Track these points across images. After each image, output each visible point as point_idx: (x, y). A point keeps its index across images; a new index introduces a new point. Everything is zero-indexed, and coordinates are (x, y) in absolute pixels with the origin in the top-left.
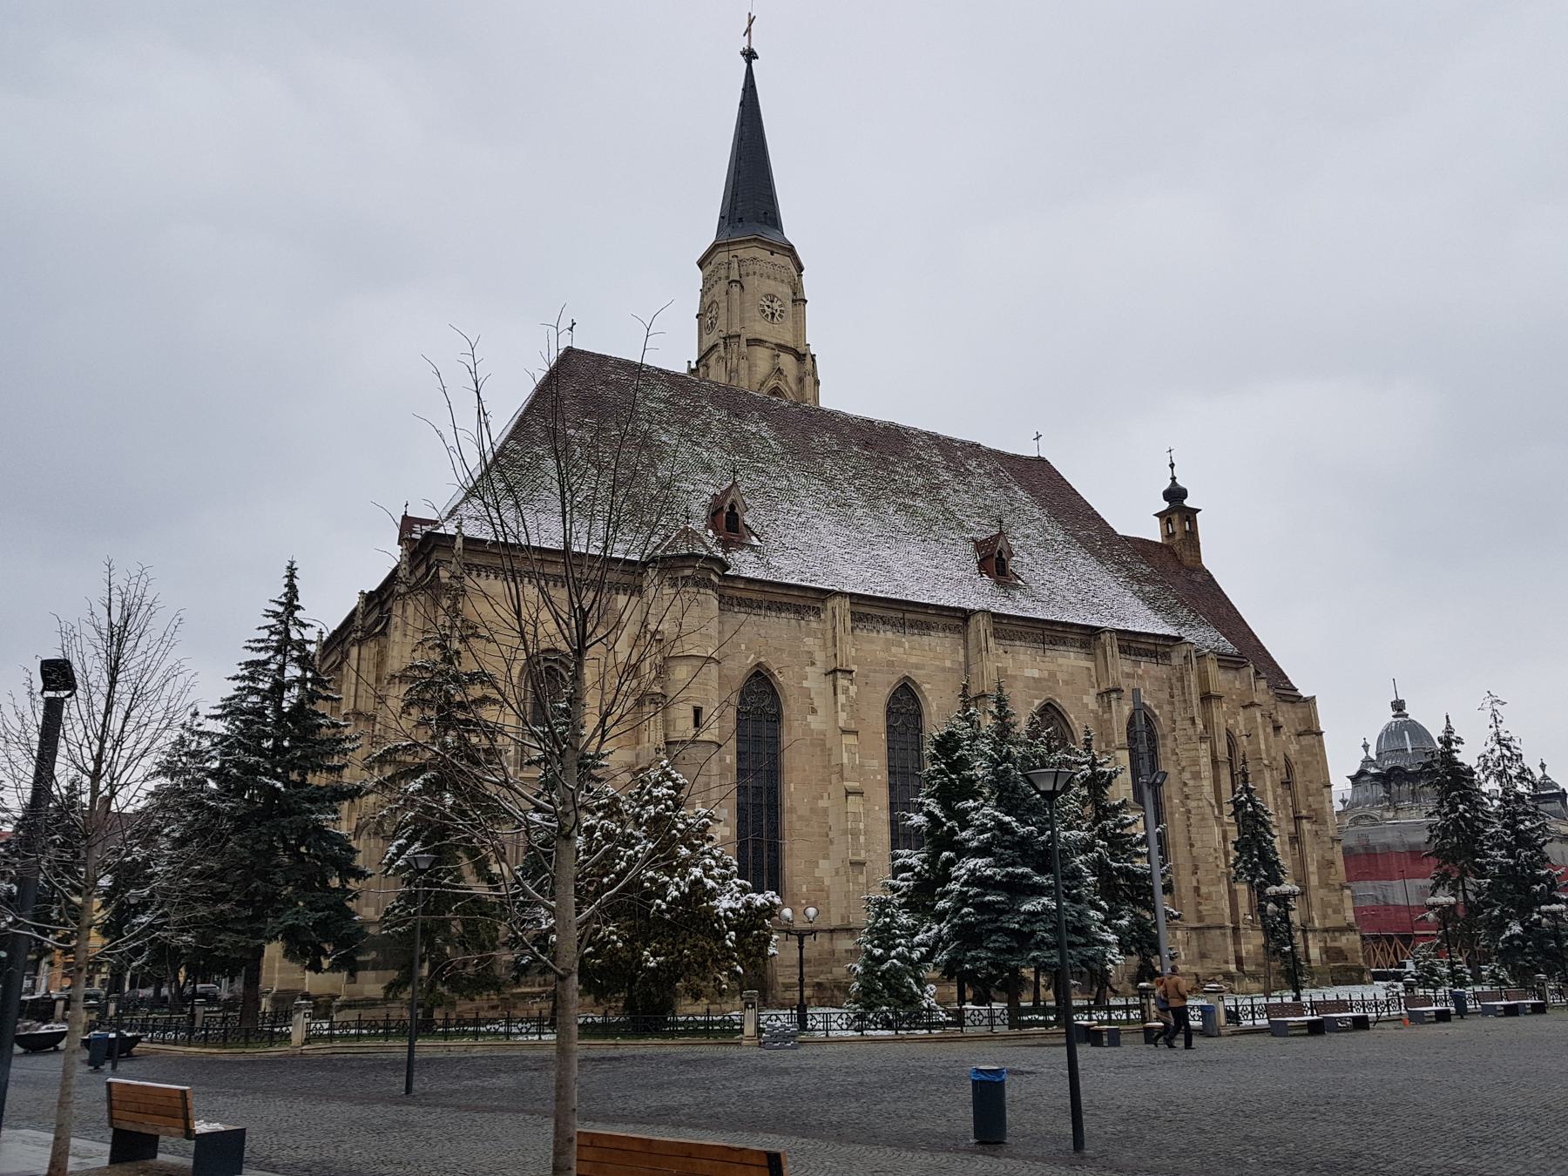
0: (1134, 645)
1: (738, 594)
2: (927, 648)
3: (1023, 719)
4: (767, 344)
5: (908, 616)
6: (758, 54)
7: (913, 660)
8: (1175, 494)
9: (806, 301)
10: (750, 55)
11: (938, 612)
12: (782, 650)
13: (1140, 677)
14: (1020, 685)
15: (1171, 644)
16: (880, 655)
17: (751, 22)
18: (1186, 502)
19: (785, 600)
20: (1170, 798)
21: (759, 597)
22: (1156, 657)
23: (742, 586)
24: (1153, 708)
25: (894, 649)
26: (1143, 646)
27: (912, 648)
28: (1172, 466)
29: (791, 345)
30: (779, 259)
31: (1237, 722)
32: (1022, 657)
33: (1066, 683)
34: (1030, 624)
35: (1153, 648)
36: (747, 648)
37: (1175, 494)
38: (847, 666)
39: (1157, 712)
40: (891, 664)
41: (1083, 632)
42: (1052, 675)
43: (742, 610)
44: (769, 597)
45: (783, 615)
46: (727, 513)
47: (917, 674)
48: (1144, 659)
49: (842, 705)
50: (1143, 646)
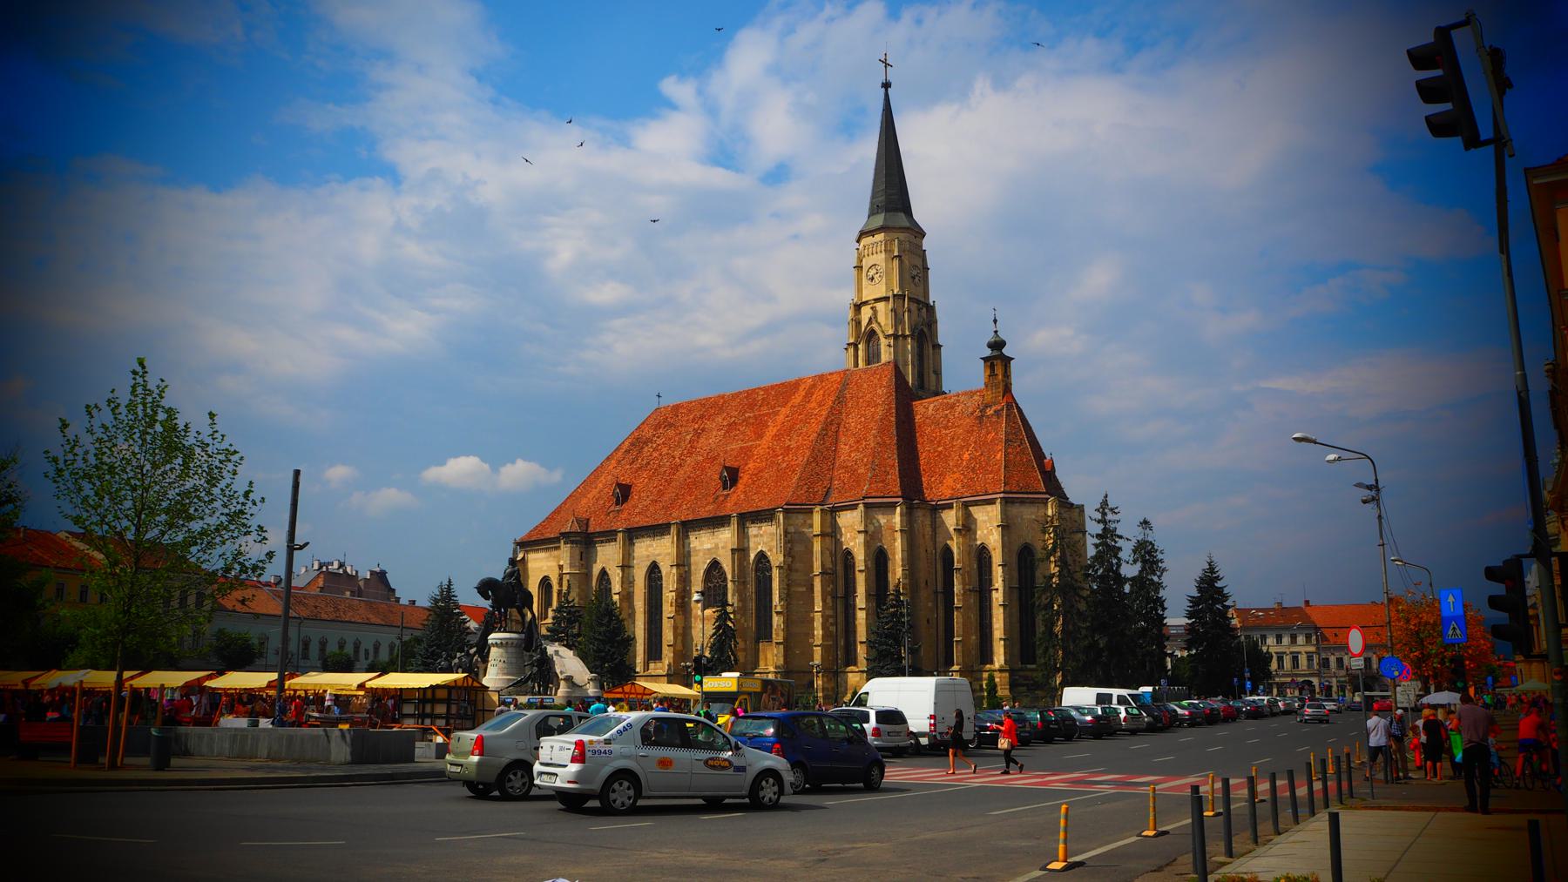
3: (702, 571)
7: (657, 552)
8: (998, 345)
10: (886, 85)
12: (609, 560)
13: (761, 535)
14: (701, 554)
16: (645, 553)
18: (1006, 351)
25: (650, 549)
28: (995, 321)
29: (884, 295)
31: (855, 543)
33: (723, 548)
37: (998, 345)
39: (769, 554)
40: (648, 556)
42: (717, 545)
47: (658, 559)
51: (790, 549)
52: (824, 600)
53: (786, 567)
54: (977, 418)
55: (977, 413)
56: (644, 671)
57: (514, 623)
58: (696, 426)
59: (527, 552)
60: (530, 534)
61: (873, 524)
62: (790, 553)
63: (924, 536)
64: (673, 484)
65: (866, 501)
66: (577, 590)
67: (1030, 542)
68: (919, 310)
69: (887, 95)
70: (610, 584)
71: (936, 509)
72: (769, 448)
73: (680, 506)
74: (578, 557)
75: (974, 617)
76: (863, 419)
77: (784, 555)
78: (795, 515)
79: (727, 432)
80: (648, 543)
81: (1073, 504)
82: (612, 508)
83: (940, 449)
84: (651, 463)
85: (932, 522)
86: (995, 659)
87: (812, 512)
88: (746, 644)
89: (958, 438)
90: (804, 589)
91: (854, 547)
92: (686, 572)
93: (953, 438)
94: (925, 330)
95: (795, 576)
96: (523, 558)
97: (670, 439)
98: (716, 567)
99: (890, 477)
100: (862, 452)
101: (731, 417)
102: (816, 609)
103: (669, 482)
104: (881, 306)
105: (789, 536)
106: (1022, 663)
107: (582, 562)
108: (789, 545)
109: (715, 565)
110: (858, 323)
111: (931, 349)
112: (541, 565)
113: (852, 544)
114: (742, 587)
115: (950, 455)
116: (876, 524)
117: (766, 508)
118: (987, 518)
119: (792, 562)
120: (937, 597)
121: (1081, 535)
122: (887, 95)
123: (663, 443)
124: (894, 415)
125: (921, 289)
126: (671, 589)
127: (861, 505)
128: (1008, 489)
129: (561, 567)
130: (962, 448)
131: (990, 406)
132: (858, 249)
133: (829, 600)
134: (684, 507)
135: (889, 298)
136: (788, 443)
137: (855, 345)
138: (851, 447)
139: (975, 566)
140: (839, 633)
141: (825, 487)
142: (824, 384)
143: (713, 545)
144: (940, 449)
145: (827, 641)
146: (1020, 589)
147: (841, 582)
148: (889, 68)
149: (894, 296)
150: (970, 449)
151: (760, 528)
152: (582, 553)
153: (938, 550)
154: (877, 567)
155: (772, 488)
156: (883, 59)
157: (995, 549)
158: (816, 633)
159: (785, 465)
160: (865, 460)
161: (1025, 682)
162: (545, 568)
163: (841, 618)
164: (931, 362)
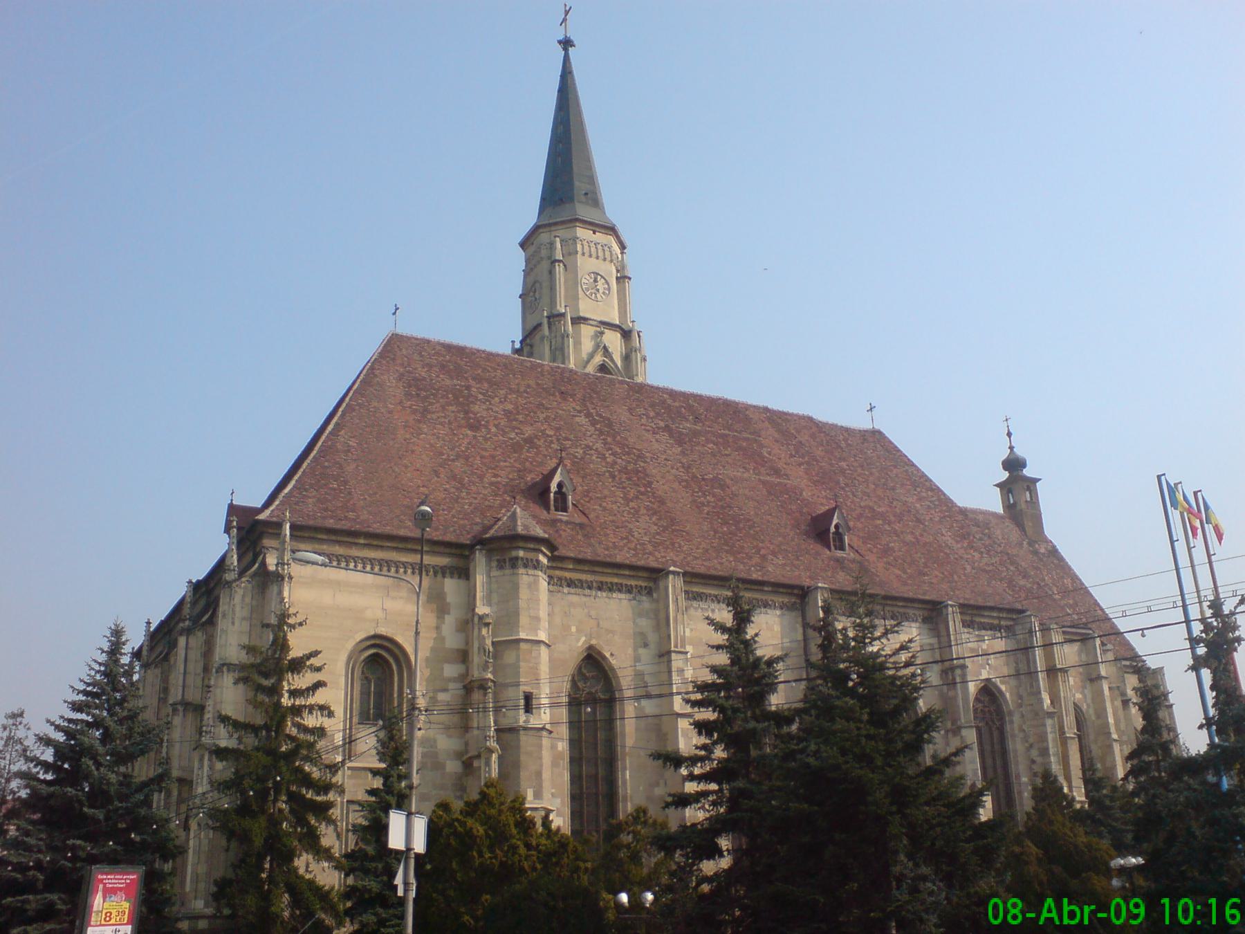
0: (978, 619)
4: (591, 322)
6: (575, 43)
8: (1013, 464)
9: (630, 278)
10: (566, 43)
11: (775, 589)
12: (613, 632)
15: (1014, 617)
17: (567, 13)
19: (616, 580)
20: (1018, 776)
21: (589, 577)
22: (1000, 631)
24: (999, 684)
26: (986, 620)
28: (1009, 434)
30: (600, 237)
35: (996, 622)
36: (578, 630)
37: (1013, 464)
38: (681, 647)
39: (1003, 688)
41: (924, 606)
43: (573, 590)
45: (615, 595)
46: (555, 493)
50: (986, 620)
69: (566, 59)
122: (566, 59)
162: (380, 614)
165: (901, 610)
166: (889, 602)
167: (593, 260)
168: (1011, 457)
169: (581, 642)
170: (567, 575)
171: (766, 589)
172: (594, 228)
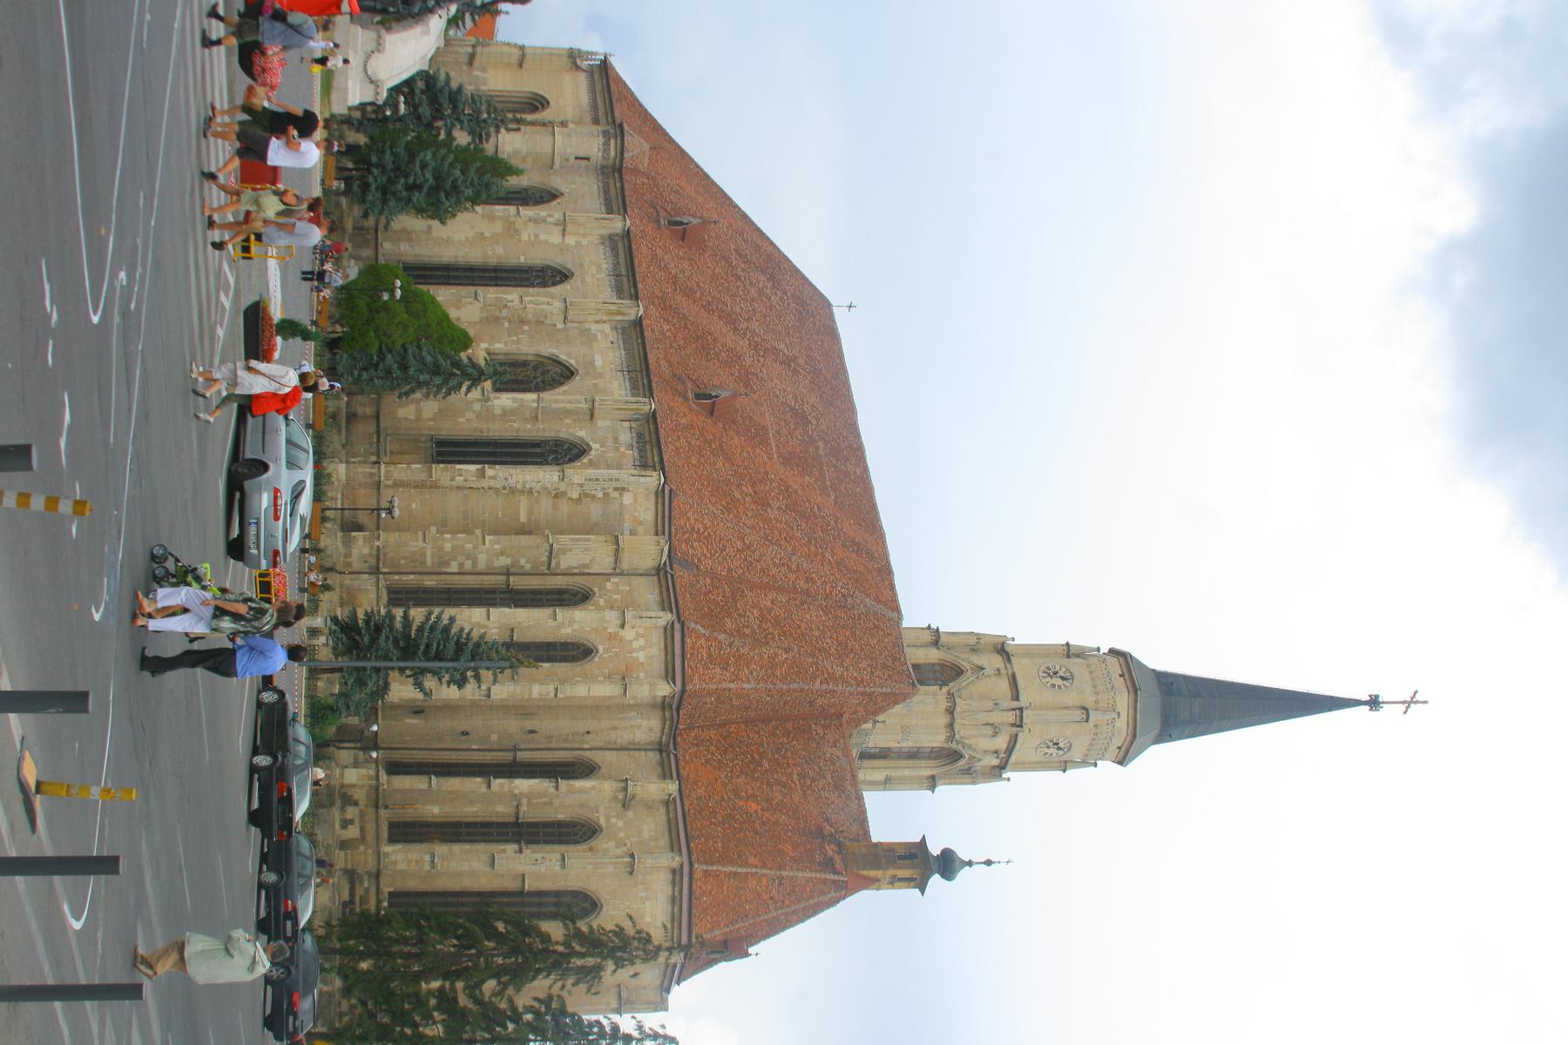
0: (648, 447)
1: (612, 186)
2: (601, 289)
3: (555, 351)
5: (625, 279)
7: (588, 279)
8: (948, 864)
10: (1374, 703)
12: (576, 203)
13: (617, 449)
18: (936, 880)
23: (618, 185)
24: (588, 457)
25: (593, 268)
26: (649, 454)
27: (598, 280)
28: (989, 863)
31: (601, 609)
32: (611, 354)
33: (595, 385)
34: (642, 359)
35: (650, 463)
37: (948, 864)
39: (585, 460)
40: (582, 265)
42: (600, 376)
44: (614, 200)
48: (636, 454)
49: (538, 214)
50: (649, 454)
51: (593, 497)
52: (502, 553)
53: (562, 489)
54: (820, 830)
55: (828, 829)
56: (383, 255)
57: (470, 50)
58: (801, 361)
59: (590, 72)
60: (619, 80)
61: (636, 639)
62: (586, 495)
63: (615, 728)
64: (705, 315)
65: (677, 626)
66: (524, 150)
67: (605, 909)
68: (996, 752)
70: (534, 205)
71: (661, 751)
72: (767, 473)
73: (667, 320)
74: (581, 154)
75: (472, 811)
76: (817, 634)
77: (581, 485)
78: (653, 508)
79: (792, 409)
80: (605, 266)
81: (668, 991)
82: (662, 213)
83: (766, 764)
84: (739, 284)
85: (639, 743)
86: (399, 846)
87: (657, 534)
88: (430, 420)
89: (785, 795)
90: (523, 519)
91: (596, 604)
92: (555, 325)
93: (784, 787)
94: (961, 763)
95: (546, 504)
96: (578, 68)
97: (779, 317)
98: (562, 375)
99: (718, 670)
100: (760, 627)
101: (817, 419)
102: (488, 538)
103: (707, 307)
104: (1004, 686)
105: (616, 494)
106: (390, 893)
107: (572, 159)
108: (600, 495)
109: (567, 373)
110: (974, 650)
111: (929, 772)
112: (570, 96)
113: (602, 602)
114: (527, 415)
115: (756, 780)
116: (635, 645)
117: (665, 458)
118: (646, 835)
119: (570, 498)
120: (509, 750)
121: (614, 1004)
123: (772, 307)
124: (824, 687)
125: (1032, 757)
126: (525, 299)
127: (670, 615)
128: (698, 874)
129: (563, 124)
130: (769, 801)
131: (839, 853)
132: (1098, 649)
133: (504, 561)
134: (666, 327)
135: (1017, 699)
136: (776, 505)
137: (936, 643)
138: (770, 610)
139: (561, 817)
140: (446, 577)
141: (699, 560)
142: (875, 574)
143: (601, 371)
144: (766, 764)
145: (433, 556)
146: (521, 893)
147: (533, 583)
148: (1402, 707)
149: (1021, 709)
150: (767, 815)
151: (631, 447)
152: (588, 159)
153: (588, 754)
154: (562, 644)
155: (699, 472)
156: (1418, 697)
157: (591, 849)
158: (448, 536)
159: (737, 495)
160: (747, 631)
161: (357, 898)
163: (472, 581)
164: (907, 773)
165: (641, 387)
166: (644, 373)
167: (1087, 676)
168: (957, 863)
169: (564, 189)
170: (612, 186)
171: (632, 290)
172: (1126, 672)
